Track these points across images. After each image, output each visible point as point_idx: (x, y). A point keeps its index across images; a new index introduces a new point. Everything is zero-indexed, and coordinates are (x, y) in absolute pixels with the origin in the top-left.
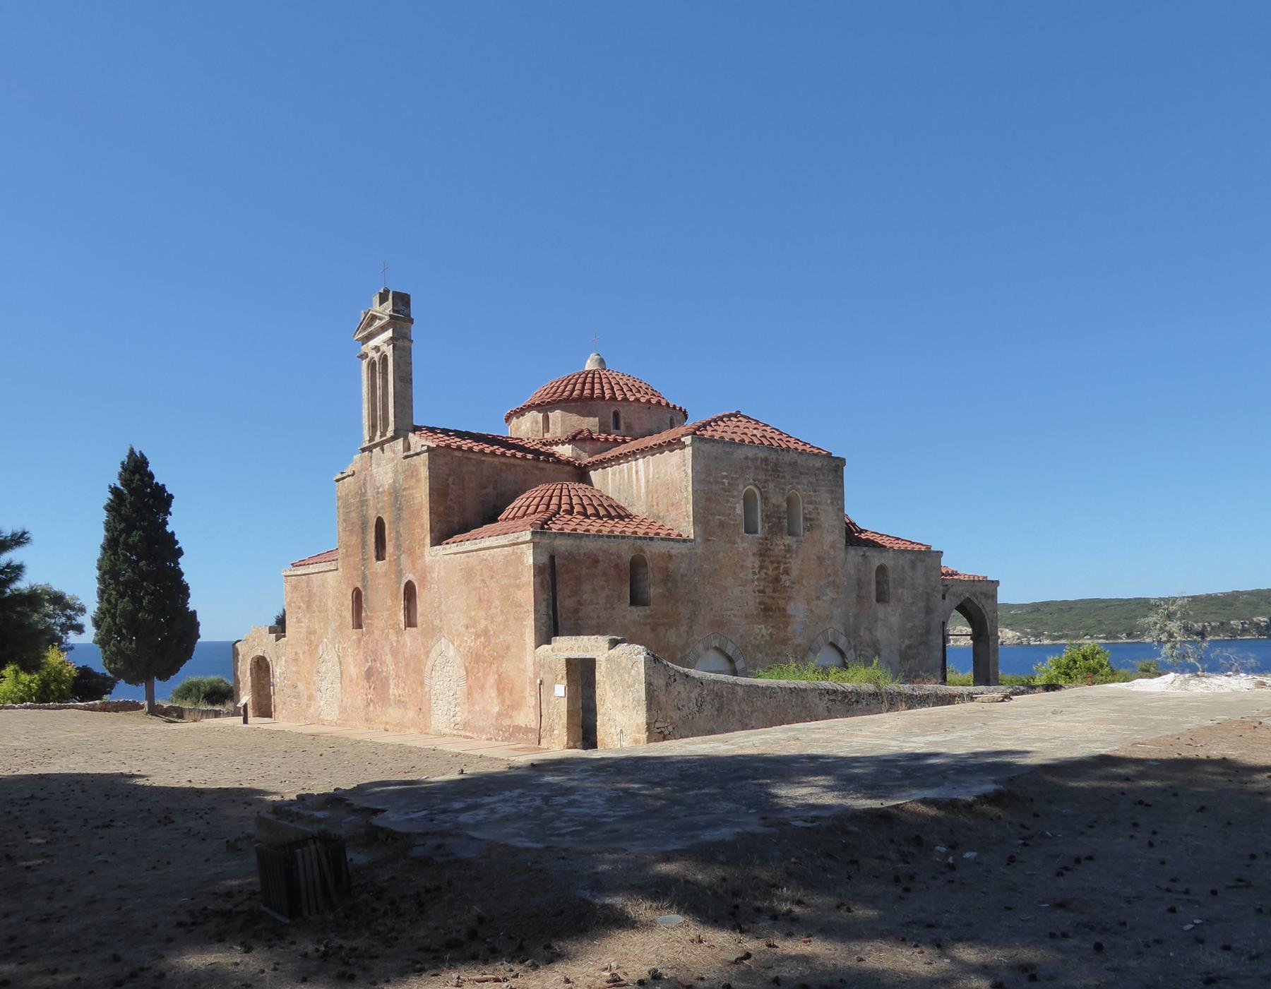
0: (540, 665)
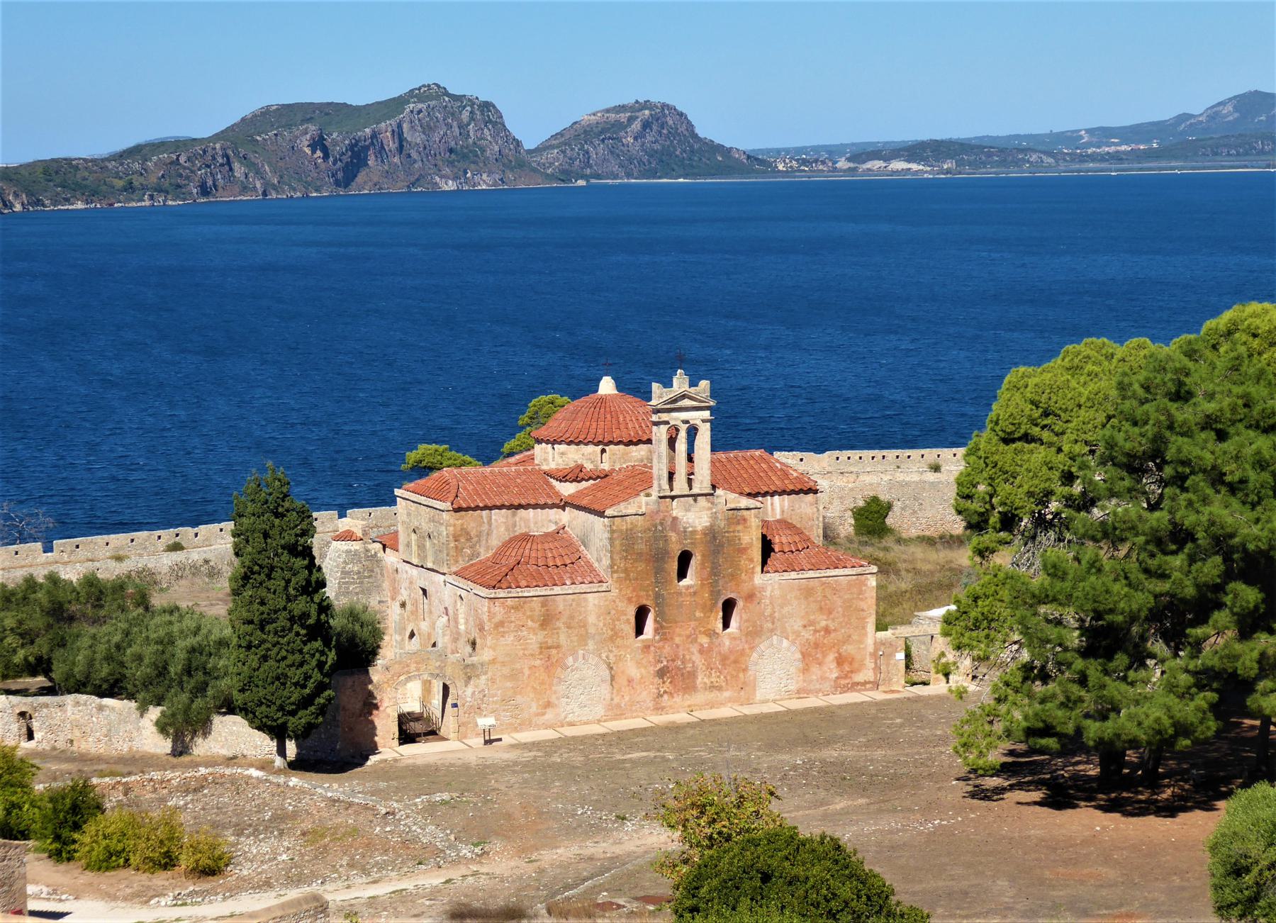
0: (879, 644)
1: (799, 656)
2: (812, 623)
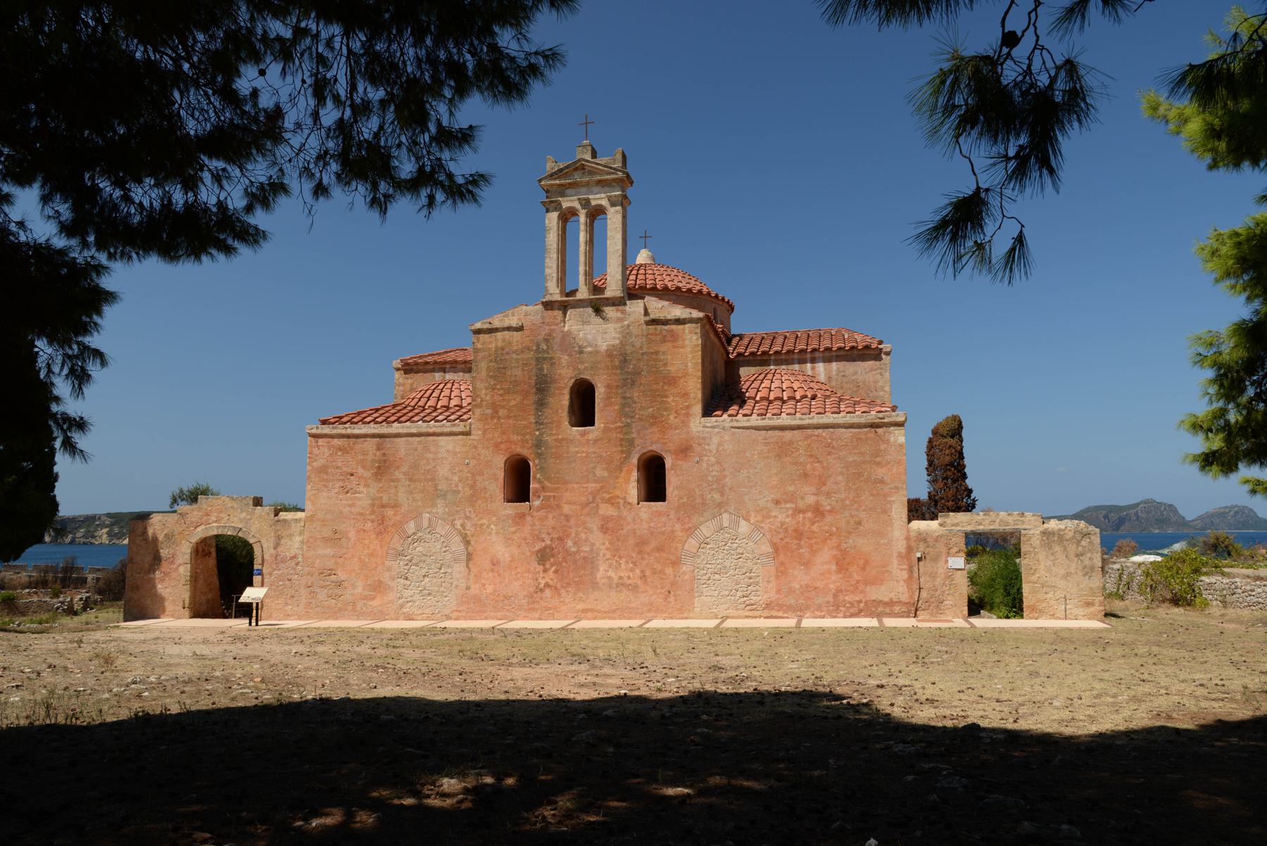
1: (767, 548)
2: (792, 498)
